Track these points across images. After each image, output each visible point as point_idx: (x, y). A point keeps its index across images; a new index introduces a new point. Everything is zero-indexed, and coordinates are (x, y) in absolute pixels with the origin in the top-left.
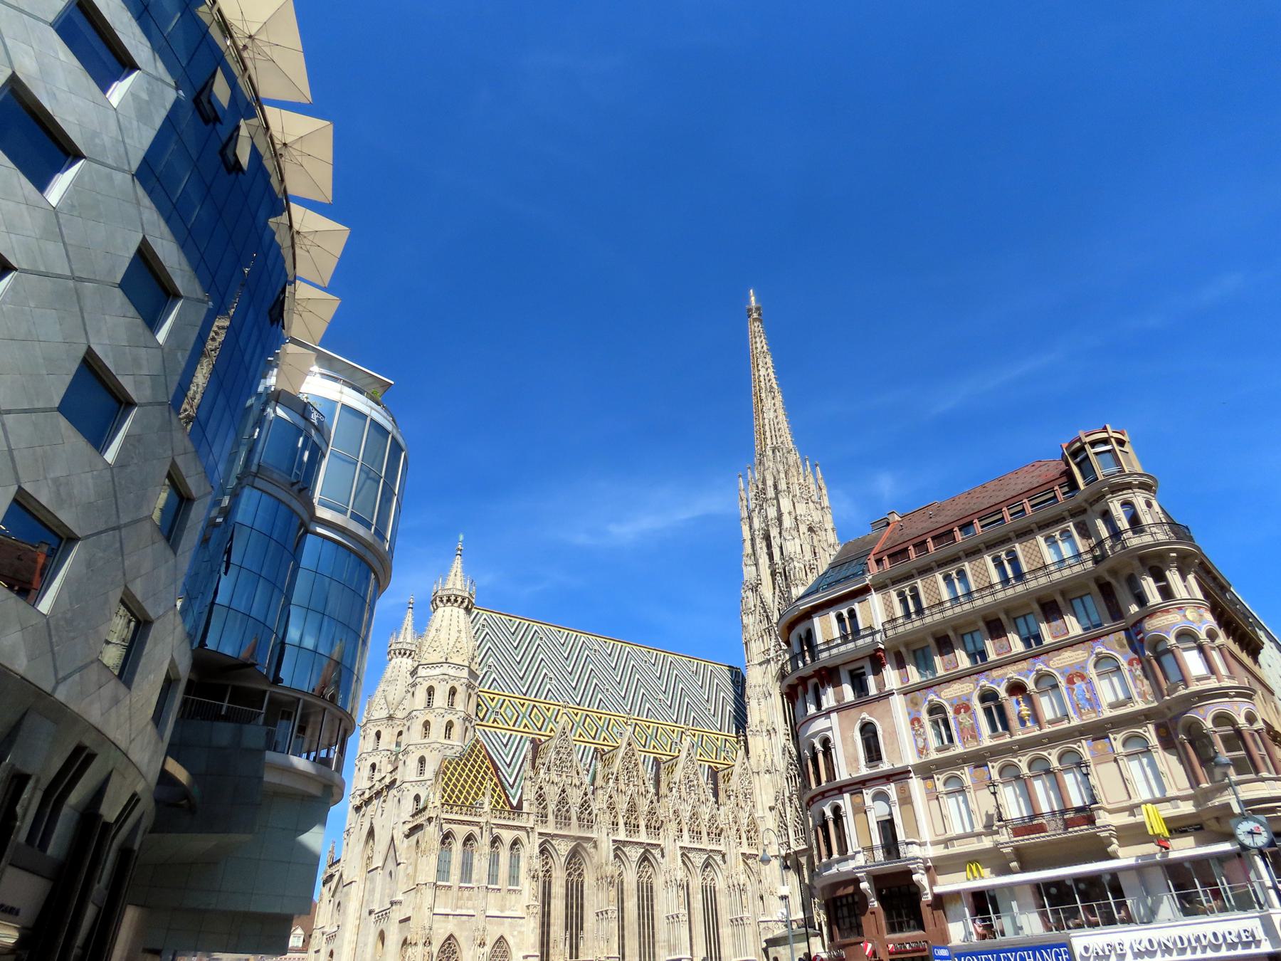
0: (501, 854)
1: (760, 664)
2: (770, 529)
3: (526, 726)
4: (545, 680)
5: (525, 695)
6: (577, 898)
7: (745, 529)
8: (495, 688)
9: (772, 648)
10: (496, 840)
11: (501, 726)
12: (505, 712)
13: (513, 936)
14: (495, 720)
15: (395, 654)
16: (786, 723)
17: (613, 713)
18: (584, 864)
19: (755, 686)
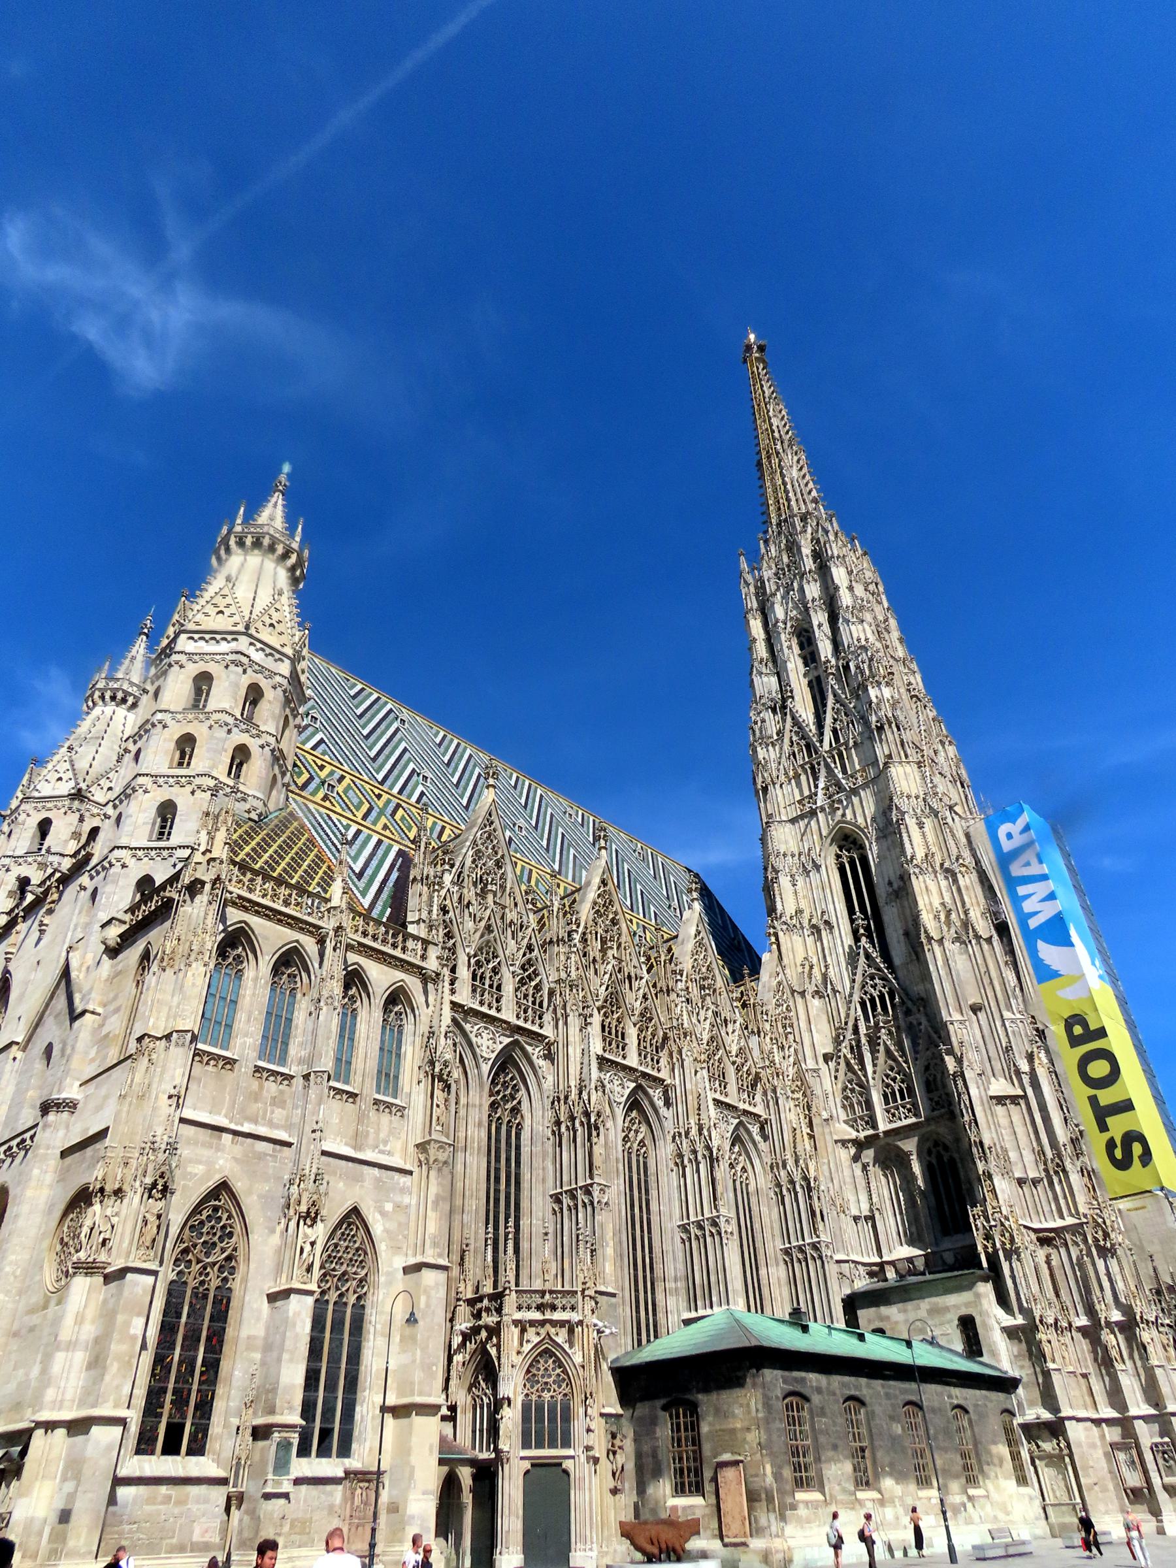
0: (362, 1015)
1: (793, 821)
2: (812, 613)
3: (385, 827)
4: (415, 778)
5: (382, 783)
6: (508, 1160)
7: (756, 627)
8: (324, 753)
9: (820, 793)
10: (354, 979)
11: (338, 809)
12: (345, 791)
13: (383, 1214)
14: (326, 798)
15: (102, 697)
16: (851, 911)
17: (533, 863)
18: (523, 1091)
19: (785, 855)
